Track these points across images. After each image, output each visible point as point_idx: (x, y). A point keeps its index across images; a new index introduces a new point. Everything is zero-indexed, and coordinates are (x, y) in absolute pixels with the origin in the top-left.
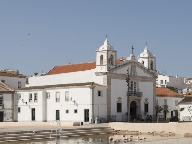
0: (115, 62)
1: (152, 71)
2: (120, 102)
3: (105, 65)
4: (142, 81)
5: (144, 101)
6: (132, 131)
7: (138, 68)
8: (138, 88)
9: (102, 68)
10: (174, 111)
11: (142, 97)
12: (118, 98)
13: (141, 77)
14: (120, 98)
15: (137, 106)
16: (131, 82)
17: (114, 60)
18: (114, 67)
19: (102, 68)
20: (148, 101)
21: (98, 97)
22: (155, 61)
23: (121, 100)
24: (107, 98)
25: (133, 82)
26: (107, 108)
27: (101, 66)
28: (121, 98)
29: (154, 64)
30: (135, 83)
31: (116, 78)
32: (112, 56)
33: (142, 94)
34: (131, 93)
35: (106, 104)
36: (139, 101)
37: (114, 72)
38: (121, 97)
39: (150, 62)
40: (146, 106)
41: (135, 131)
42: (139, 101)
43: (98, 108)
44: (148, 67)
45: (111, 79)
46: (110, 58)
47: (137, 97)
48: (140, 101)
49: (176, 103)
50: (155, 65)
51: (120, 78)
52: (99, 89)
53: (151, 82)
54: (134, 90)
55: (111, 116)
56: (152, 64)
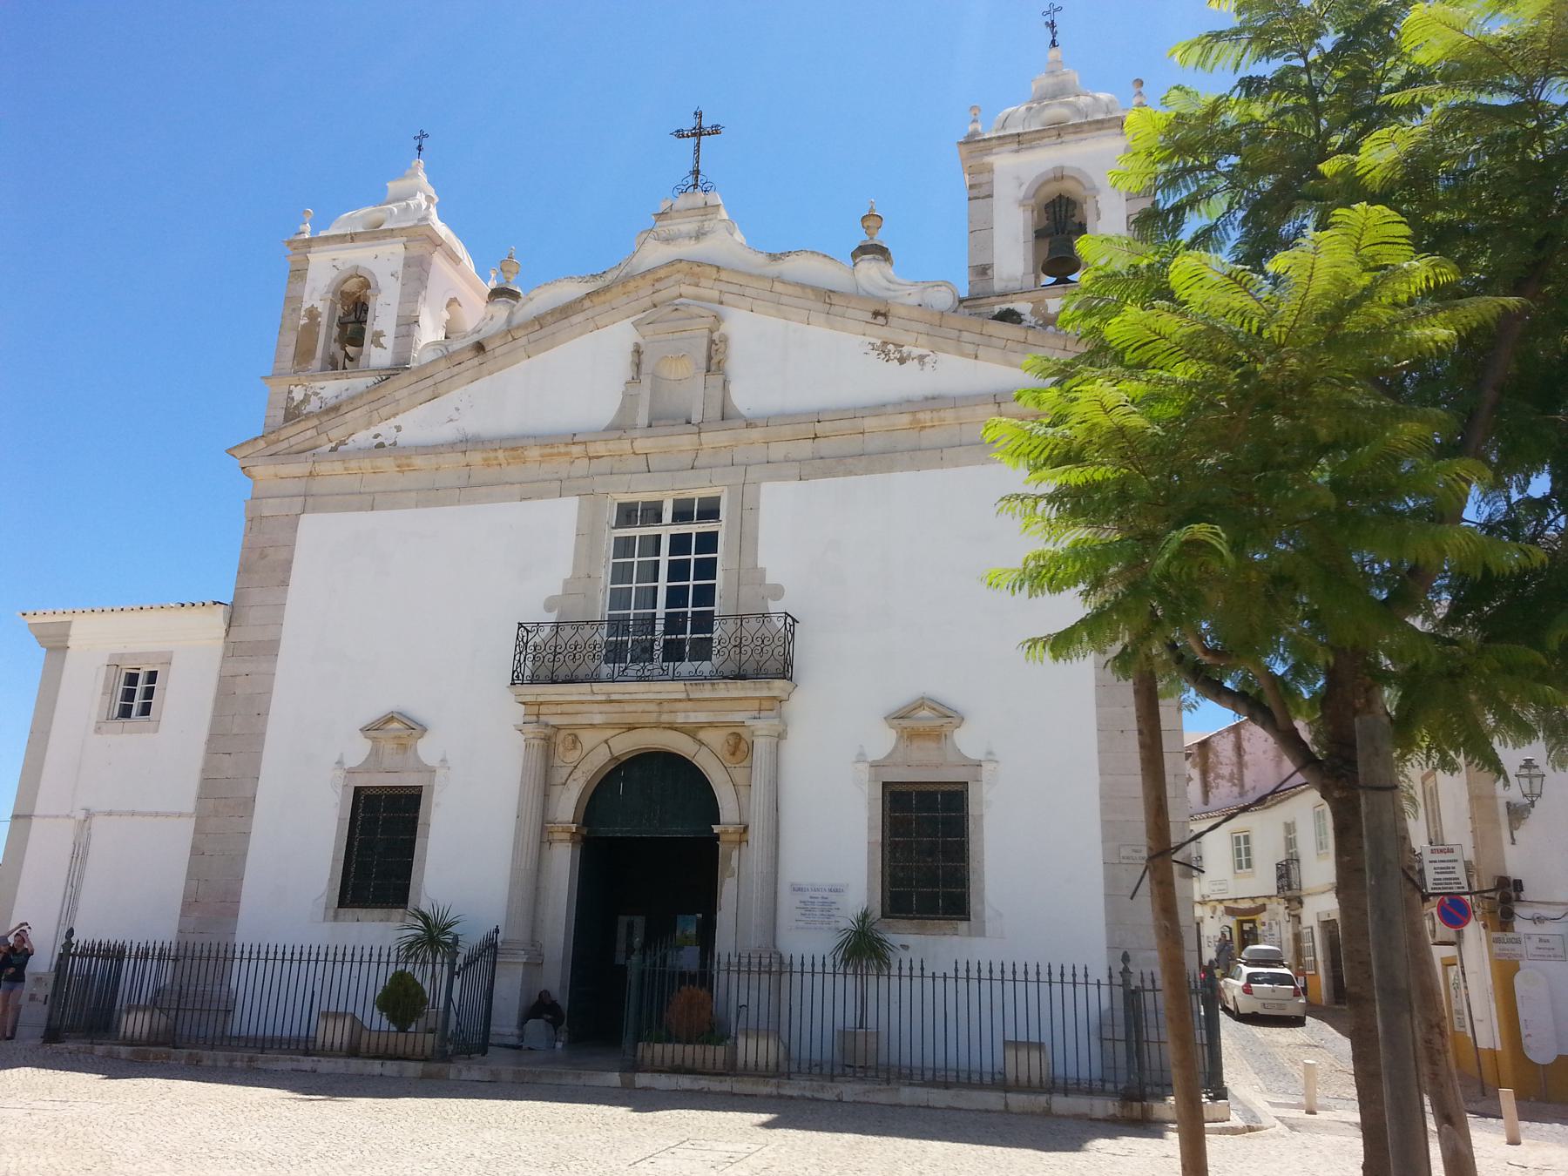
2: (409, 780)
14: (397, 728)
21: (98, 730)
23: (427, 750)
24: (213, 738)
26: (196, 851)
28: (415, 728)
34: (615, 653)
35: (189, 804)
43: (79, 855)
51: (432, 495)
52: (118, 648)
55: (223, 957)
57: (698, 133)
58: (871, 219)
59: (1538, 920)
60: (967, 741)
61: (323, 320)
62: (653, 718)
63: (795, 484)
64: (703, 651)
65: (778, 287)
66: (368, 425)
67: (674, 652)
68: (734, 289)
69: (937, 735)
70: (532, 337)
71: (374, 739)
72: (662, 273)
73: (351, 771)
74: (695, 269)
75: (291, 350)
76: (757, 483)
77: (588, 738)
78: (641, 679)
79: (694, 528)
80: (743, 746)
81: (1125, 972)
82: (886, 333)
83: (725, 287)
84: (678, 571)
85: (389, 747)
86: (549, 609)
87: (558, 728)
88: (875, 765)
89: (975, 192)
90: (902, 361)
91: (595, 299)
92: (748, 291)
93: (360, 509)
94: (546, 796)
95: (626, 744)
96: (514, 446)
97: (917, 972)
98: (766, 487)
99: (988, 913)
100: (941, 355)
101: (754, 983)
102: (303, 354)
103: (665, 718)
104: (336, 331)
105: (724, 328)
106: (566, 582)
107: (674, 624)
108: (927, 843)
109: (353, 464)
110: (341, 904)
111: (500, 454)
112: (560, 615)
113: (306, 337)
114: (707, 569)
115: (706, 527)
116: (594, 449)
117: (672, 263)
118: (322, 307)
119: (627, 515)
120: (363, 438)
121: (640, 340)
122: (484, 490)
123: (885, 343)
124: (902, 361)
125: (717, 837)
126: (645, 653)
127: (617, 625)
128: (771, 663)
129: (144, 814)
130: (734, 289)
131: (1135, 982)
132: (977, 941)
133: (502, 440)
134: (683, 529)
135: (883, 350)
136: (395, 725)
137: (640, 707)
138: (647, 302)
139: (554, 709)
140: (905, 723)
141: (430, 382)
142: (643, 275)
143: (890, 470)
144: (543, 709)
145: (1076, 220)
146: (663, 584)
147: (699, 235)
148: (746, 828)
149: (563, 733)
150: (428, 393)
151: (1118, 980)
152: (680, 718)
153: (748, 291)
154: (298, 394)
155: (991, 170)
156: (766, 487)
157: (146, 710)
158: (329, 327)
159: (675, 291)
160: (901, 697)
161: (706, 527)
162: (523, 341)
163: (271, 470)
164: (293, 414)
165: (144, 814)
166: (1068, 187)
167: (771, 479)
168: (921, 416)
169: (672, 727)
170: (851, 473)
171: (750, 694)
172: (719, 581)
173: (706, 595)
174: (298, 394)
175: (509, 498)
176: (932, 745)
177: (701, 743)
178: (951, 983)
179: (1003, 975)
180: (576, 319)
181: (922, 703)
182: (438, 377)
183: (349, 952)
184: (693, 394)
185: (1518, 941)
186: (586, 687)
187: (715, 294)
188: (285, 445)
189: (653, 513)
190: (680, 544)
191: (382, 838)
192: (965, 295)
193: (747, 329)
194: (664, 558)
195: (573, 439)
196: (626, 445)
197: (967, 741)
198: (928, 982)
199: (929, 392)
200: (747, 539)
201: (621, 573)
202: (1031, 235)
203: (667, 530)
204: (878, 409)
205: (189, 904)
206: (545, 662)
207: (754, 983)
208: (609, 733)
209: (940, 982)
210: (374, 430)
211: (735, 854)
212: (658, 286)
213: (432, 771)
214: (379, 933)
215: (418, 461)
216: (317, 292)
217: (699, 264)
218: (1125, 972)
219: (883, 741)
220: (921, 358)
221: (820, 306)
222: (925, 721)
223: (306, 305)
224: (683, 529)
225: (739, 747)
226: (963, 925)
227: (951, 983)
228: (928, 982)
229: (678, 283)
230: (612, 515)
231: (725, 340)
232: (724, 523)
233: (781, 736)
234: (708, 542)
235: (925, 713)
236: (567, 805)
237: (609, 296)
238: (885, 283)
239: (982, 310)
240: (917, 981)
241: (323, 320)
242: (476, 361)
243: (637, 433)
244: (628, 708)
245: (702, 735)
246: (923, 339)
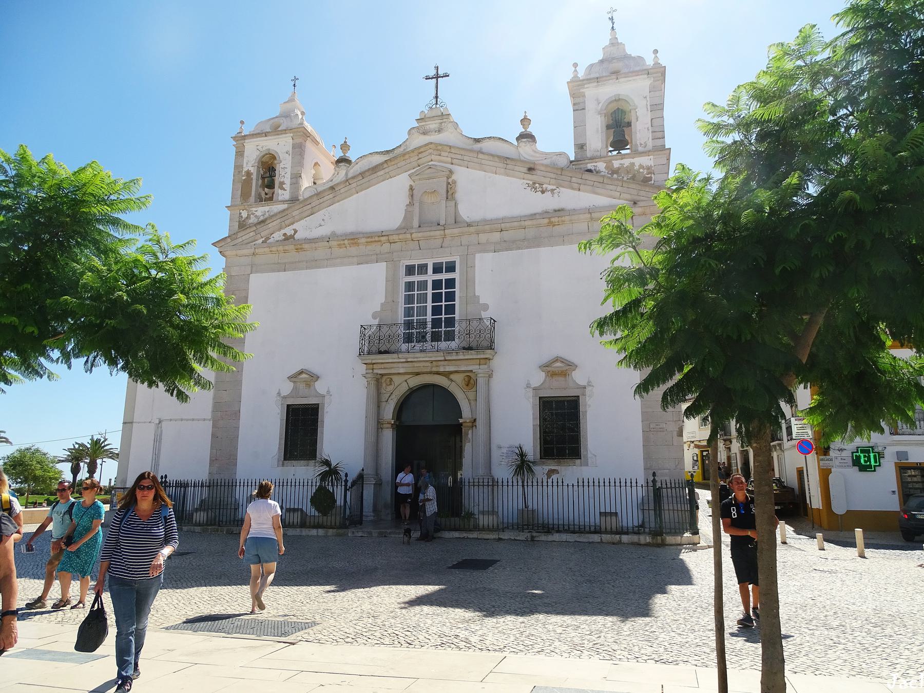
1: (616, 164)
12: (293, 378)
14: (305, 377)
26: (214, 436)
28: (315, 377)
34: (408, 339)
35: (209, 415)
38: (316, 370)
44: (580, 147)
57: (437, 77)
58: (525, 121)
59: (841, 450)
60: (579, 377)
61: (254, 177)
62: (428, 370)
63: (491, 254)
64: (450, 337)
65: (481, 156)
66: (280, 230)
67: (436, 337)
68: (459, 157)
69: (564, 374)
70: (359, 183)
71: (294, 382)
72: (422, 150)
73: (285, 397)
74: (439, 148)
75: (239, 192)
76: (474, 255)
77: (397, 380)
78: (421, 351)
79: (444, 276)
80: (472, 381)
81: (654, 481)
82: (535, 178)
83: (453, 156)
84: (436, 298)
85: (302, 386)
86: (374, 317)
87: (382, 375)
88: (534, 389)
89: (577, 107)
90: (543, 192)
91: (390, 164)
92: (466, 158)
94: (379, 407)
95: (415, 382)
96: (353, 239)
97: (560, 483)
98: (478, 256)
99: (589, 455)
100: (562, 189)
101: (481, 490)
102: (245, 195)
103: (434, 369)
104: (260, 181)
105: (454, 177)
106: (382, 305)
107: (436, 323)
108: (561, 426)
109: (274, 249)
110: (285, 459)
111: (346, 242)
112: (380, 321)
113: (246, 184)
114: (451, 297)
115: (450, 276)
116: (391, 238)
117: (426, 145)
118: (253, 170)
119: (410, 270)
120: (278, 236)
121: (412, 183)
122: (339, 260)
123: (534, 183)
124: (543, 192)
125: (461, 424)
126: (422, 338)
127: (408, 325)
128: (483, 343)
129: (187, 420)
130: (459, 157)
131: (658, 485)
132: (584, 468)
133: (346, 235)
134: (438, 277)
135: (533, 187)
136: (304, 376)
137: (422, 364)
138: (415, 164)
139: (380, 366)
140: (549, 369)
141: (309, 206)
142: (413, 151)
143: (539, 246)
145: (626, 120)
146: (429, 304)
147: (439, 131)
148: (475, 420)
149: (385, 378)
150: (309, 212)
151: (651, 484)
152: (442, 369)
153: (466, 158)
154: (244, 214)
155: (584, 96)
156: (478, 256)
158: (257, 180)
159: (429, 158)
160: (546, 357)
161: (450, 276)
162: (354, 185)
163: (234, 253)
164: (243, 225)
165: (187, 420)
166: (626, 107)
167: (480, 252)
168: (553, 220)
169: (438, 373)
170: (519, 248)
171: (475, 357)
172: (457, 302)
173: (451, 309)
174: (244, 214)
175: (352, 264)
176: (562, 379)
177: (452, 380)
178: (576, 488)
179: (596, 484)
181: (557, 359)
182: (313, 204)
183: (289, 481)
184: (441, 211)
185: (831, 460)
186: (395, 355)
187: (449, 160)
188: (240, 240)
189: (423, 269)
190: (437, 284)
191: (301, 426)
192: (572, 158)
193: (464, 176)
194: (430, 292)
195: (382, 234)
196: (408, 236)
197: (579, 377)
198: (565, 488)
199: (557, 208)
200: (469, 282)
201: (409, 299)
202: (605, 128)
203: (430, 277)
204: (533, 216)
206: (376, 345)
207: (481, 490)
208: (407, 377)
209: (570, 488)
210: (283, 231)
211: (470, 432)
212: (420, 156)
213: (324, 396)
214: (306, 473)
215: (306, 246)
216: (250, 164)
217: (440, 145)
218: (654, 481)
219: (538, 378)
220: (552, 190)
221: (501, 165)
222: (558, 368)
223: (245, 169)
224: (438, 277)
225: (470, 382)
226: (578, 461)
227: (576, 488)
228: (565, 488)
229: (431, 154)
230: (403, 271)
231: (454, 182)
233: (490, 376)
234: (451, 283)
235: (558, 364)
236: (388, 412)
237: (396, 161)
238: (532, 153)
239: (582, 166)
240: (560, 488)
241: (254, 177)
242: (331, 196)
243: (413, 231)
244: (416, 365)
245: (452, 377)
246: (553, 181)
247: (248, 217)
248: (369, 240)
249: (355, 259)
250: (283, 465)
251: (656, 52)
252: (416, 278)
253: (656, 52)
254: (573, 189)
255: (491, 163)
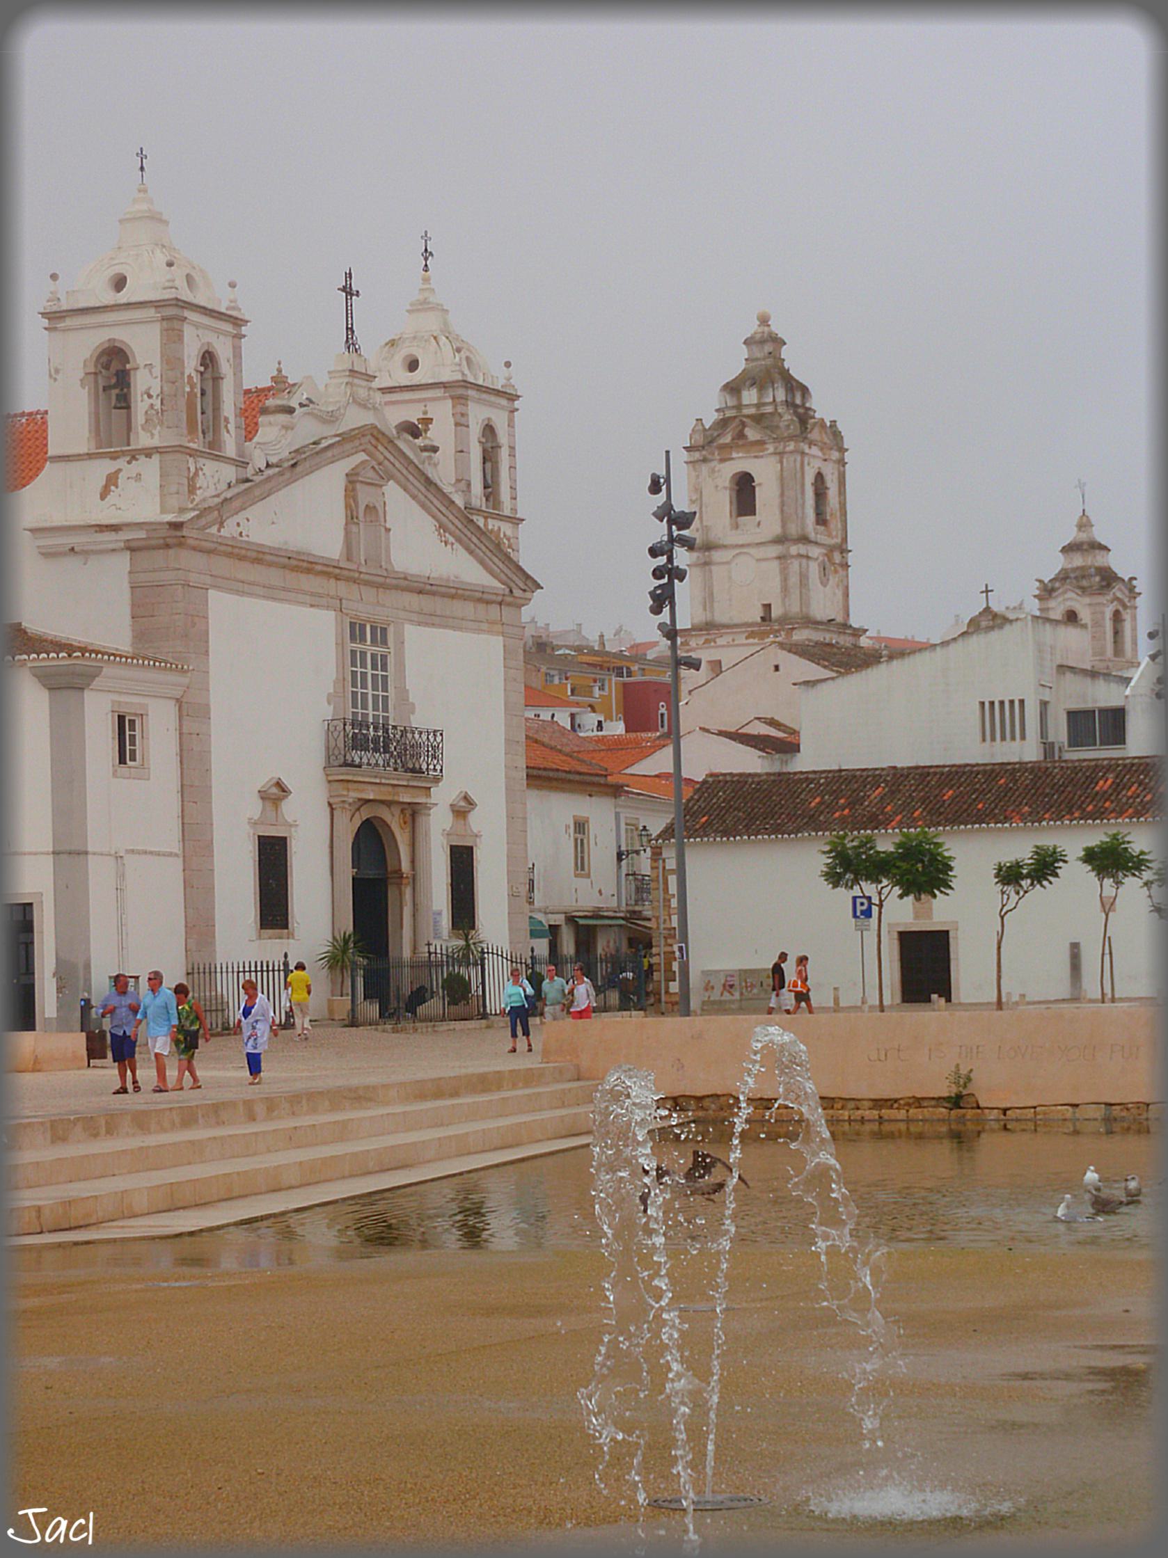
0: (231, 427)
3: (148, 453)
4: (429, 620)
5: (448, 827)
6: (878, 1103)
7: (393, 494)
8: (403, 692)
9: (112, 480)
10: (571, 919)
11: (437, 780)
13: (424, 588)
14: (276, 794)
15: (399, 871)
16: (352, 625)
17: (229, 408)
18: (230, 473)
19: (112, 480)
20: (474, 819)
21: (115, 775)
22: (511, 424)
23: (290, 808)
25: (363, 627)
27: (108, 466)
29: (504, 453)
30: (380, 635)
31: (241, 588)
32: (208, 359)
33: (435, 752)
35: (176, 848)
36: (413, 813)
37: (229, 530)
38: (286, 782)
39: (475, 431)
40: (462, 862)
41: (918, 1102)
42: (414, 815)
45: (212, 593)
46: (196, 379)
47: (403, 779)
48: (421, 820)
49: (576, 840)
50: (512, 467)
51: (271, 593)
53: (489, 632)
54: (375, 708)
56: (489, 457)
68: (392, 459)
90: (446, 543)
93: (238, 592)
130: (392, 459)
144: (350, 785)
157: (133, 759)
175: (303, 604)
180: (329, 454)
205: (189, 928)
232: (392, 650)
244: (383, 788)
247: (196, 474)
248: (325, 569)
249: (308, 599)
250: (260, 937)
251: (508, 365)
252: (358, 646)
253: (508, 365)
254: (467, 549)
255: (415, 482)
